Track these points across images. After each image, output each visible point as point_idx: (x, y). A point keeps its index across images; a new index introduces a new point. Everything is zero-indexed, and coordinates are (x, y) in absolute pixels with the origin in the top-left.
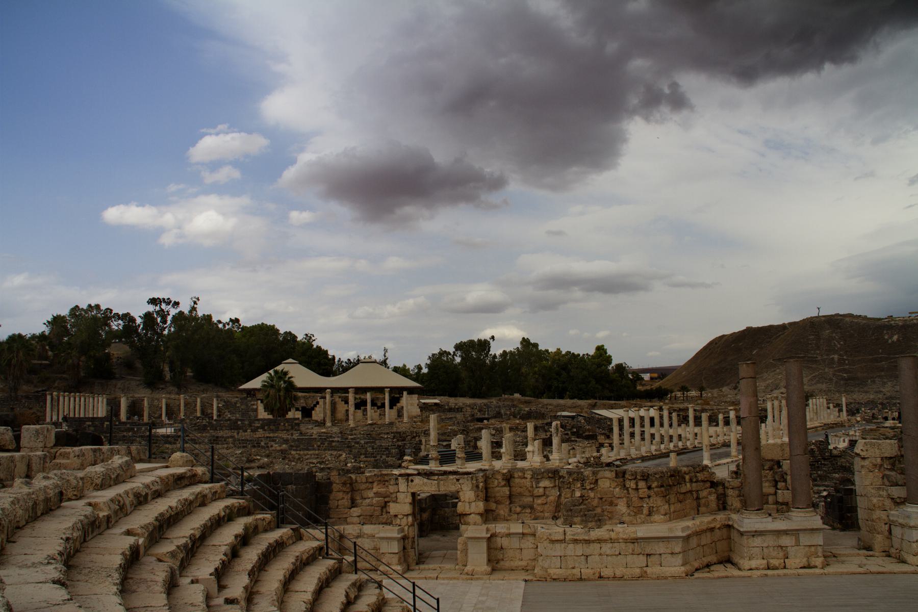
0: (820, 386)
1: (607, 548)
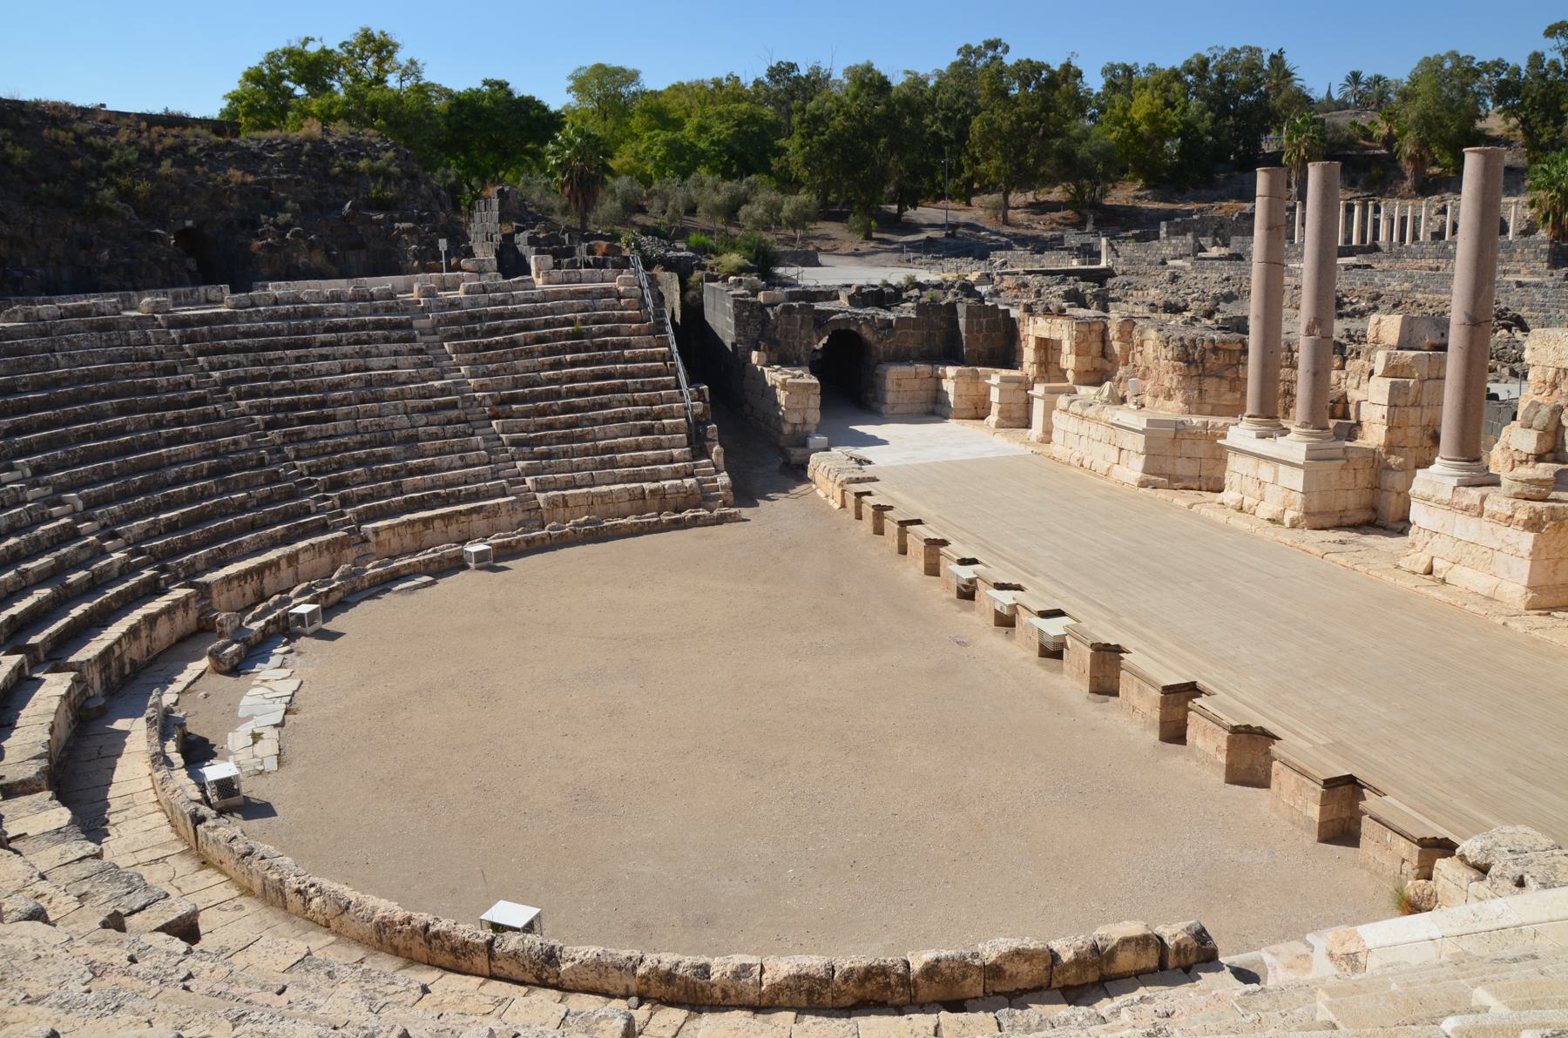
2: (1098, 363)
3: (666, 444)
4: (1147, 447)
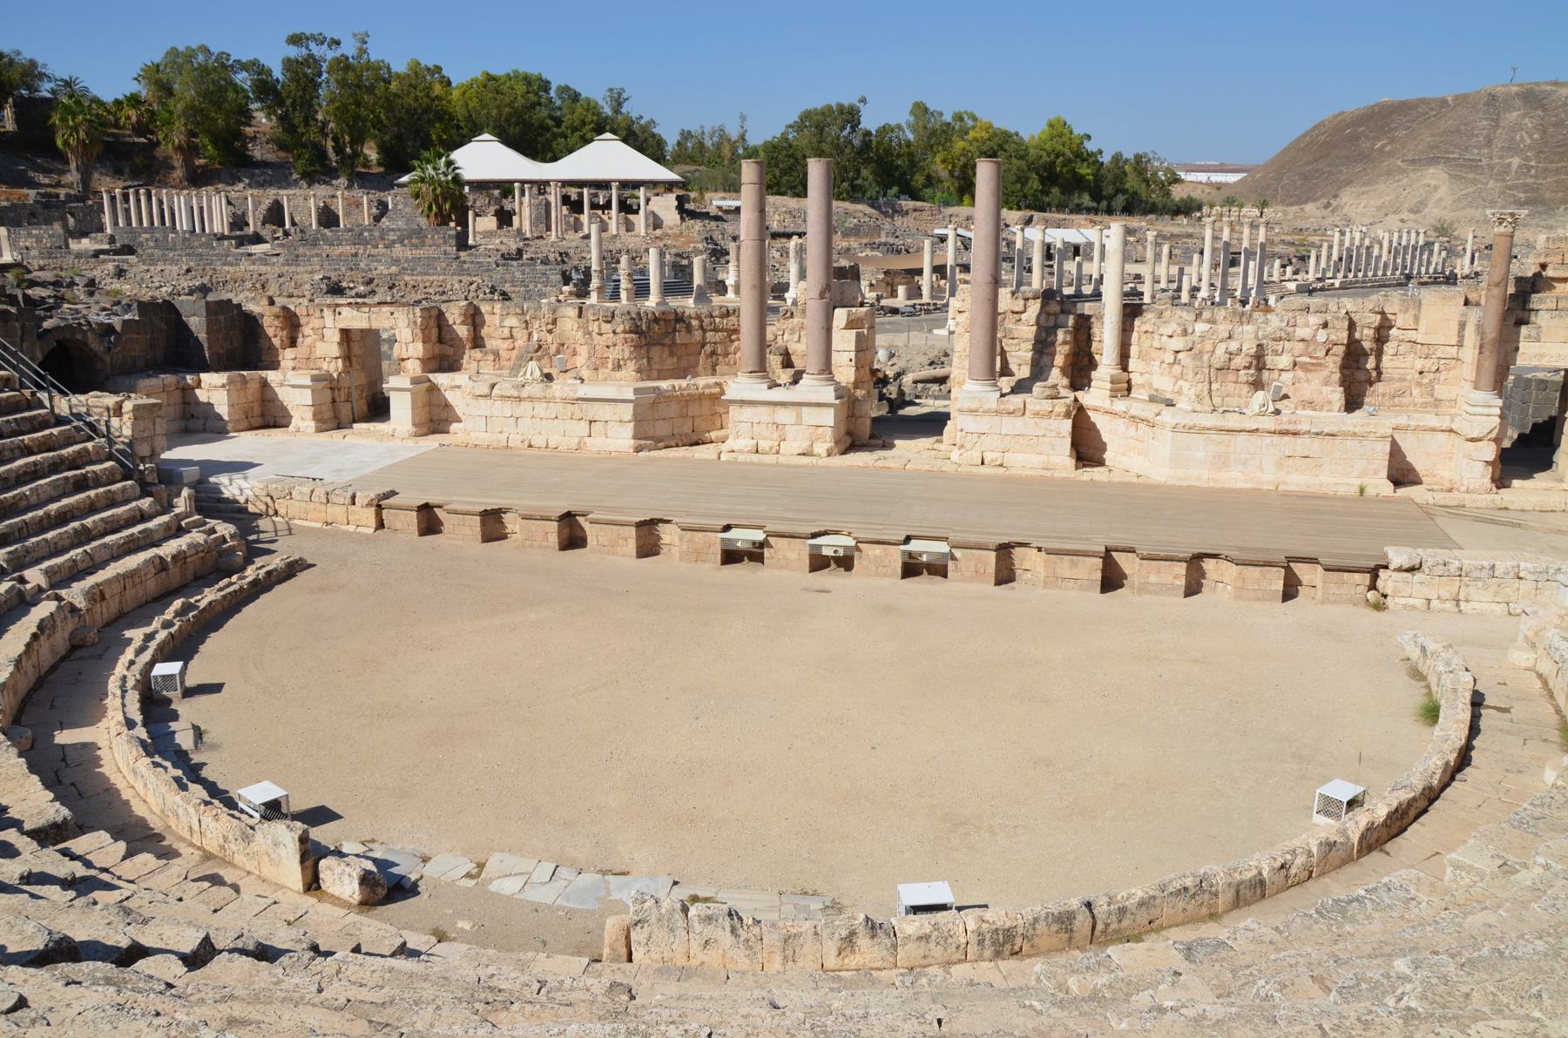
0: (1471, 212)
1: (540, 409)
2: (437, 348)
3: (119, 498)
4: (635, 415)
